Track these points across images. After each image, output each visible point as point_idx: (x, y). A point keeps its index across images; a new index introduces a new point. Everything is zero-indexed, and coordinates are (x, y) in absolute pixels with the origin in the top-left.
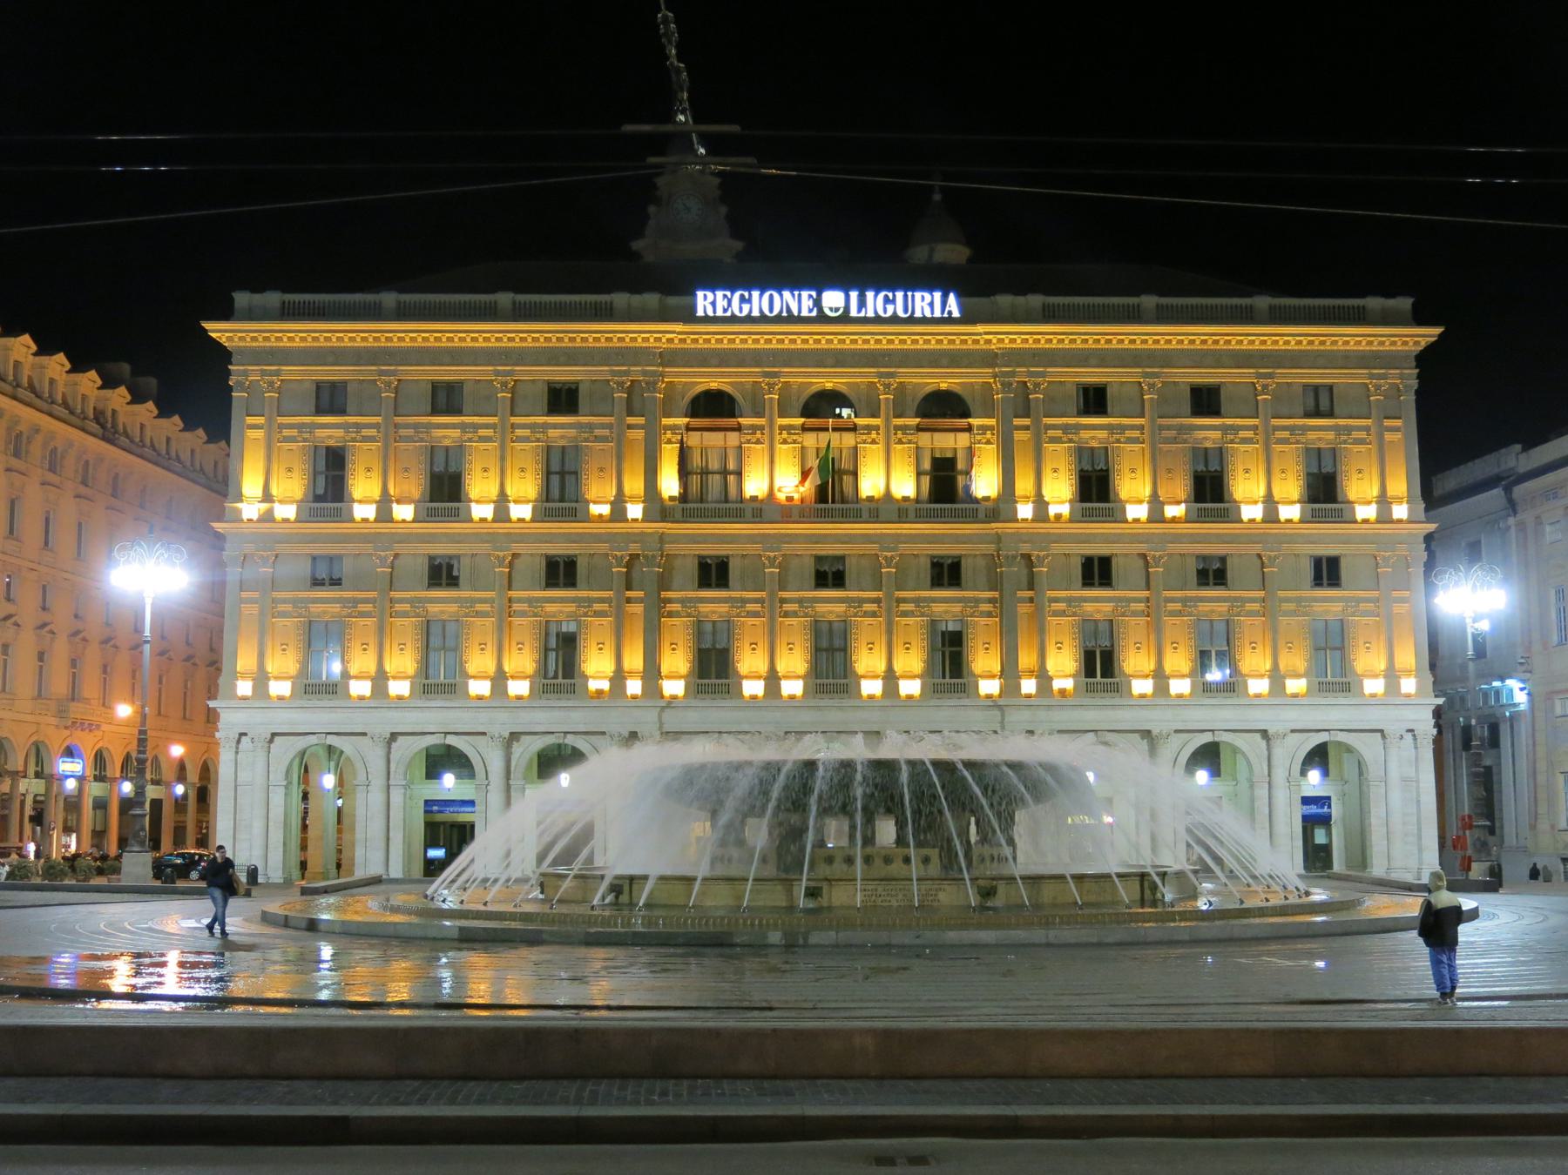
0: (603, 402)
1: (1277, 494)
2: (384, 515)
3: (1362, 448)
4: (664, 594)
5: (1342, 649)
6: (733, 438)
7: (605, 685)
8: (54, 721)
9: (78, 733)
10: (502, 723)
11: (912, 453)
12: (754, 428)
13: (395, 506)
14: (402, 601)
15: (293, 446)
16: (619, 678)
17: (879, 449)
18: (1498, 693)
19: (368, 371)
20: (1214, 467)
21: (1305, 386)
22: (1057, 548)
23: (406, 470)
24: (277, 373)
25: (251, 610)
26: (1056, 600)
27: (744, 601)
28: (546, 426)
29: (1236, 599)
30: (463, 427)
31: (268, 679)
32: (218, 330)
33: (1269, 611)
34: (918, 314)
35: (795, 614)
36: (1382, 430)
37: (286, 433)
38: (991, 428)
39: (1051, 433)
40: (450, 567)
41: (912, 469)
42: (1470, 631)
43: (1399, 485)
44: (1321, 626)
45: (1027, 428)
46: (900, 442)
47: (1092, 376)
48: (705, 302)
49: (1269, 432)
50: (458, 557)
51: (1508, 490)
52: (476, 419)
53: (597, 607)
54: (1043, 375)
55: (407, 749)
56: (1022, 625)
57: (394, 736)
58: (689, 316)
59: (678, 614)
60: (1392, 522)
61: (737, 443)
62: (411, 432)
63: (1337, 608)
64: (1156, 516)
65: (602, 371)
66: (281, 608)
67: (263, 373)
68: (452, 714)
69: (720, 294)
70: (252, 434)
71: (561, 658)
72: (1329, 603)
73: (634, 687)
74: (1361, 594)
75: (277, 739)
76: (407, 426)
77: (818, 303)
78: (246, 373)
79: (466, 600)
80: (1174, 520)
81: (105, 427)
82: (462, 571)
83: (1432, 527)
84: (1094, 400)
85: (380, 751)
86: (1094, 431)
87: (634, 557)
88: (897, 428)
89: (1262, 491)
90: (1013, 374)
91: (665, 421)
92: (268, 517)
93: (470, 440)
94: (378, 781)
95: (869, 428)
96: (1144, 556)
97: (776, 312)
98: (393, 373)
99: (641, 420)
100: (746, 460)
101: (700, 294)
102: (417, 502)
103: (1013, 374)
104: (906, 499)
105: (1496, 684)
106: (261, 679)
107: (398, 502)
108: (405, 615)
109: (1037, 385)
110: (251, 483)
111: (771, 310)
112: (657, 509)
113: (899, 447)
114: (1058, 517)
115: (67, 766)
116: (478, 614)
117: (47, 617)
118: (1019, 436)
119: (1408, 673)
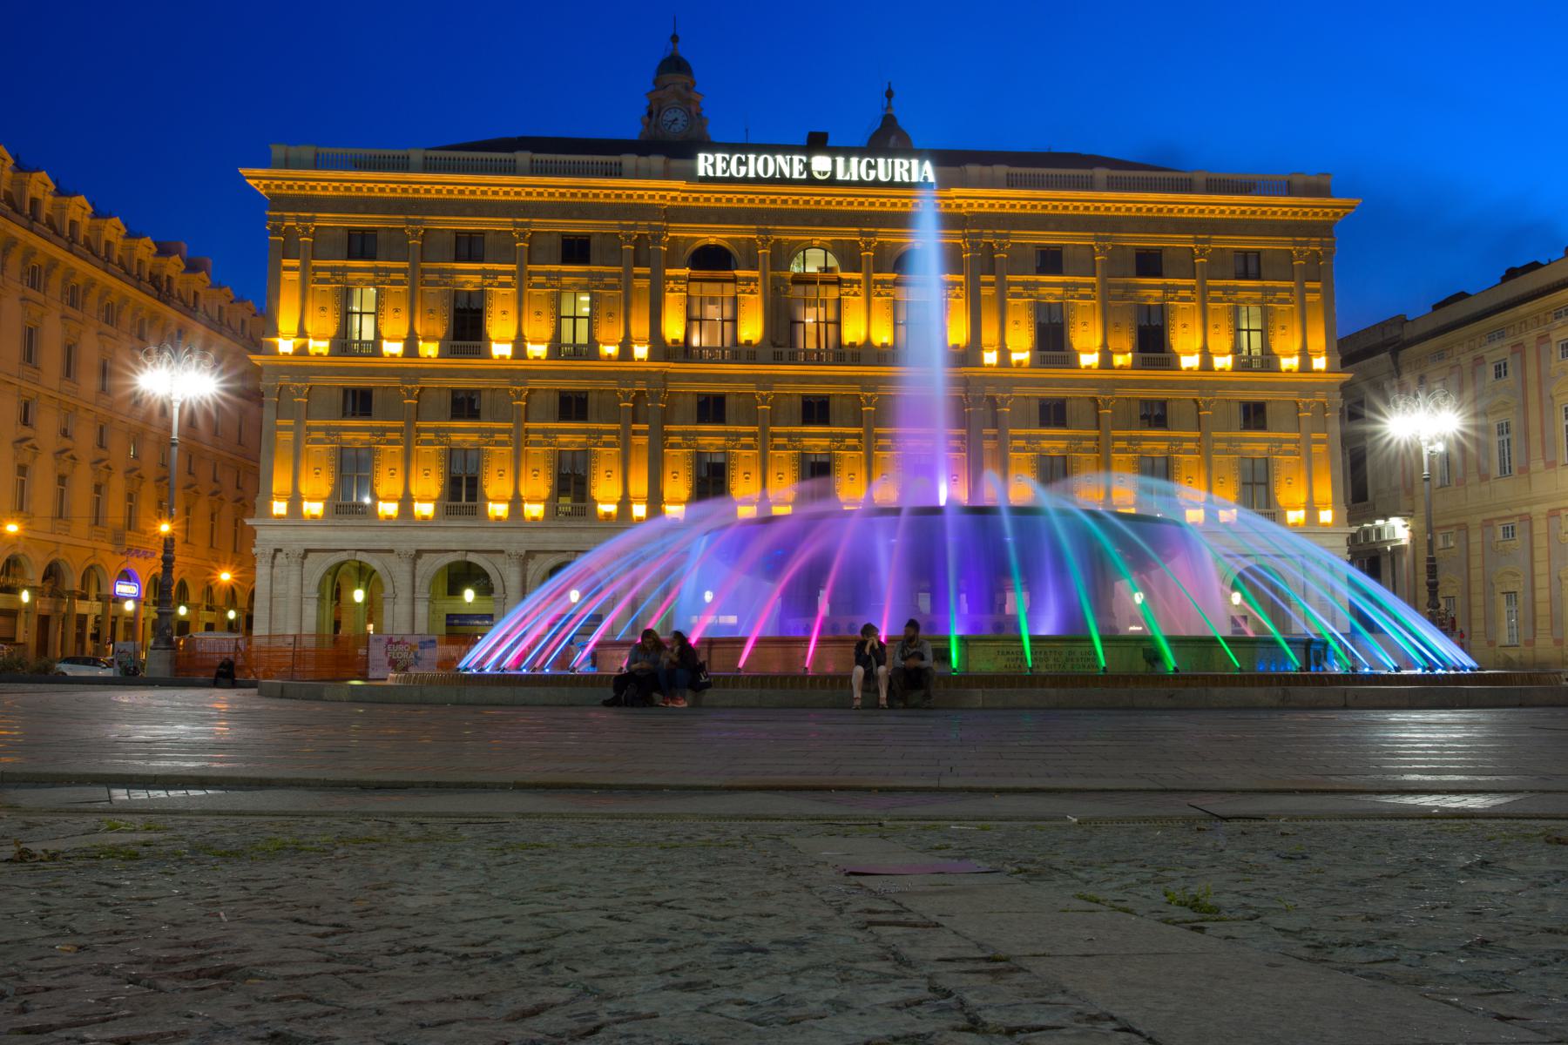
0: (612, 252)
1: (1211, 347)
2: (411, 349)
3: (1286, 307)
4: (666, 428)
5: (1267, 484)
6: (729, 289)
7: (612, 508)
8: (111, 547)
9: (135, 559)
10: (518, 543)
11: (890, 305)
12: (749, 280)
13: (421, 343)
14: (427, 430)
15: (327, 287)
16: (625, 503)
17: (861, 299)
18: (1379, 531)
19: (396, 221)
20: (1155, 322)
21: (1237, 251)
22: (1019, 392)
23: (431, 311)
24: (312, 219)
25: (287, 436)
26: (1017, 438)
27: (739, 435)
28: (560, 274)
29: (1175, 439)
30: (484, 273)
31: (302, 499)
32: (257, 178)
33: (1205, 451)
34: (897, 179)
35: (784, 447)
36: (1304, 291)
37: (320, 275)
38: (960, 284)
39: (1013, 289)
40: (472, 401)
41: (890, 319)
42: (1425, 453)
43: (1318, 340)
44: (1248, 464)
45: (991, 284)
46: (879, 295)
47: (1050, 238)
48: (705, 163)
49: (1205, 290)
50: (478, 391)
51: (1395, 355)
52: (497, 267)
53: (606, 438)
54: (1006, 236)
55: (432, 565)
56: (987, 458)
57: (419, 553)
58: (691, 176)
59: (678, 446)
60: (1312, 371)
61: (732, 294)
62: (435, 277)
63: (1262, 448)
64: (1106, 362)
65: (611, 226)
66: (316, 435)
67: (299, 219)
68: (472, 534)
69: (719, 156)
70: (286, 275)
71: (571, 483)
72: (1256, 443)
73: (639, 510)
74: (1283, 435)
75: (310, 555)
76: (432, 271)
77: (807, 166)
78: (282, 219)
79: (486, 430)
80: (1121, 367)
81: (160, 288)
82: (484, 404)
83: (1347, 376)
84: (1050, 261)
85: (406, 567)
86: (1051, 287)
87: (640, 394)
88: (877, 282)
89: (1198, 343)
90: (980, 235)
91: (669, 272)
92: (302, 351)
93: (490, 285)
94: (404, 595)
95: (852, 282)
96: (1095, 400)
97: (770, 173)
98: (420, 222)
99: (647, 270)
100: (741, 309)
101: (701, 156)
102: (442, 342)
103: (980, 235)
104: (884, 345)
105: (1379, 523)
106: (295, 501)
107: (424, 340)
108: (430, 443)
109: (1001, 246)
110: (287, 321)
111: (766, 172)
112: (660, 349)
113: (878, 299)
114: (1019, 364)
115: (123, 589)
116: (497, 443)
117: (104, 454)
118: (985, 291)
119: (1325, 506)
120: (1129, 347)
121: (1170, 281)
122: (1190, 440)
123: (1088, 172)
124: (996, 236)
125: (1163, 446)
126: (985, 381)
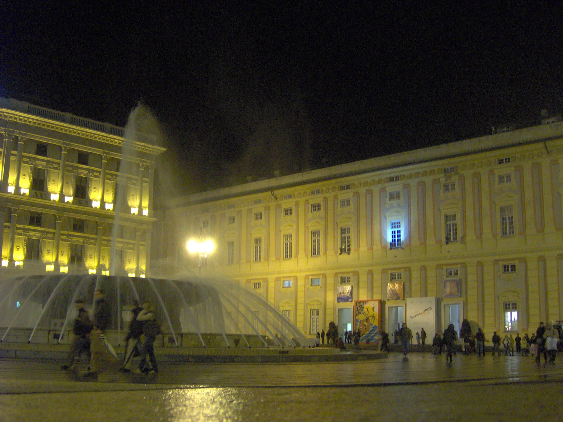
1: (105, 199)
22: (22, 207)
39: (25, 159)
43: (146, 203)
45: (15, 155)
47: (44, 140)
83: (155, 219)
84: (42, 149)
90: (13, 132)
96: (55, 216)
114: (24, 194)
118: (12, 158)
120: (71, 194)
121: (91, 168)
122: (92, 239)
123: (63, 113)
124: (20, 133)
125: (81, 240)
126: (9, 200)
